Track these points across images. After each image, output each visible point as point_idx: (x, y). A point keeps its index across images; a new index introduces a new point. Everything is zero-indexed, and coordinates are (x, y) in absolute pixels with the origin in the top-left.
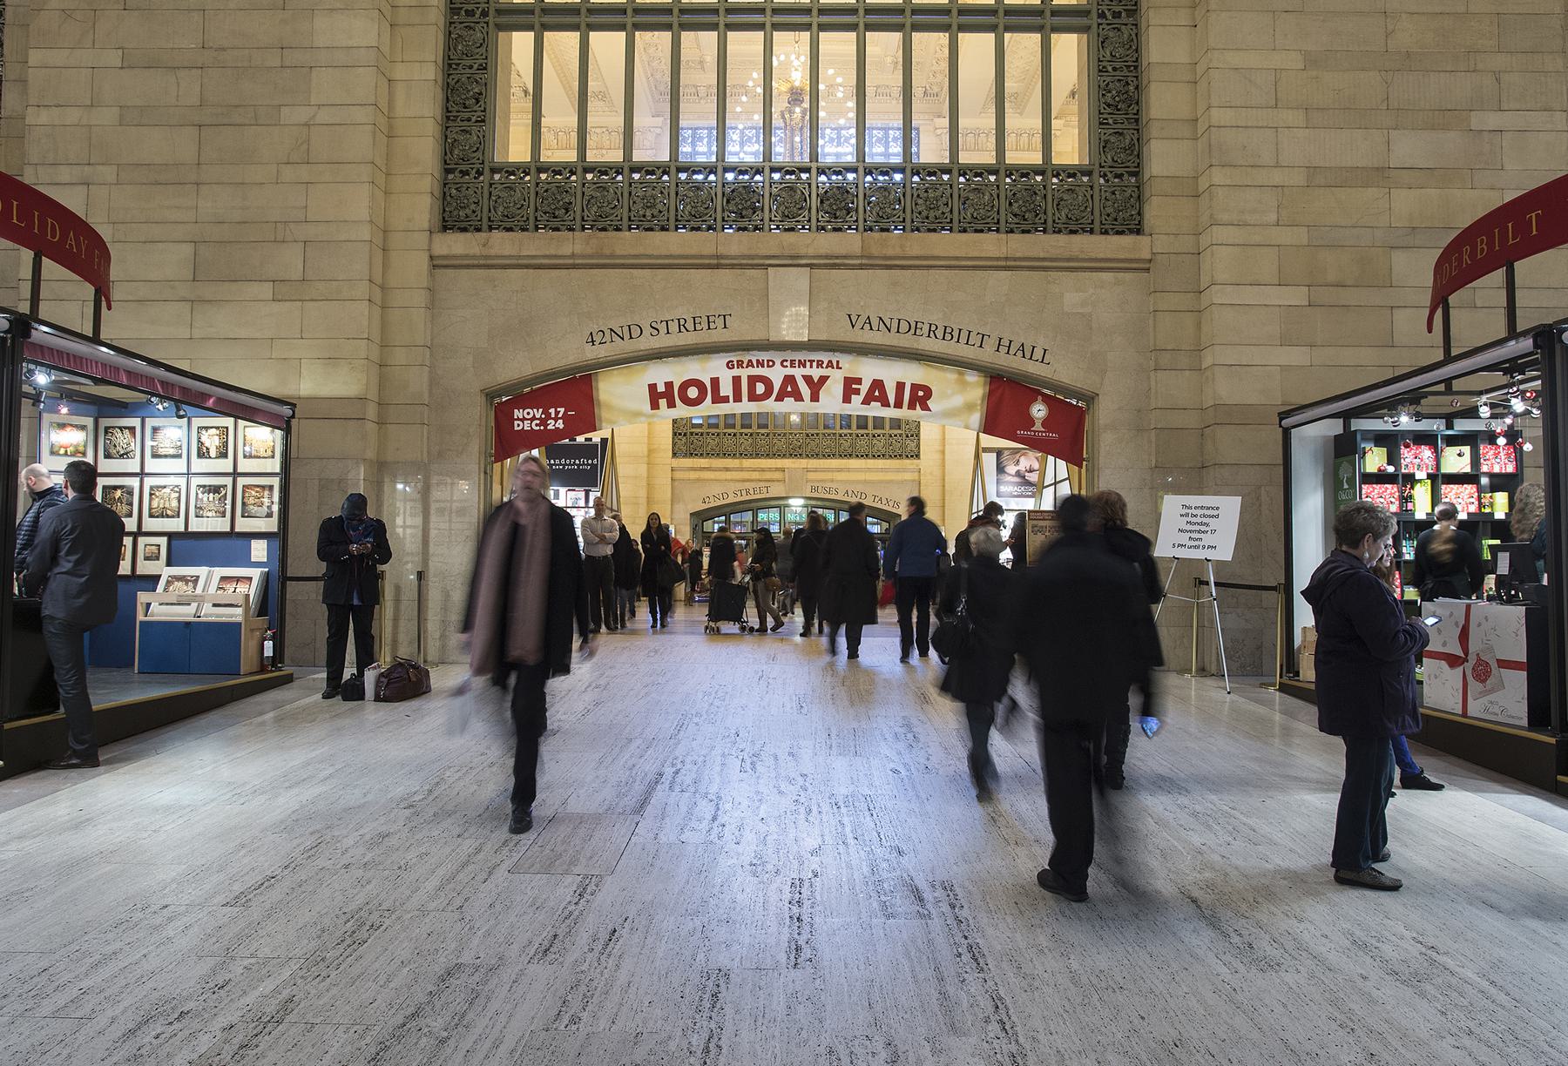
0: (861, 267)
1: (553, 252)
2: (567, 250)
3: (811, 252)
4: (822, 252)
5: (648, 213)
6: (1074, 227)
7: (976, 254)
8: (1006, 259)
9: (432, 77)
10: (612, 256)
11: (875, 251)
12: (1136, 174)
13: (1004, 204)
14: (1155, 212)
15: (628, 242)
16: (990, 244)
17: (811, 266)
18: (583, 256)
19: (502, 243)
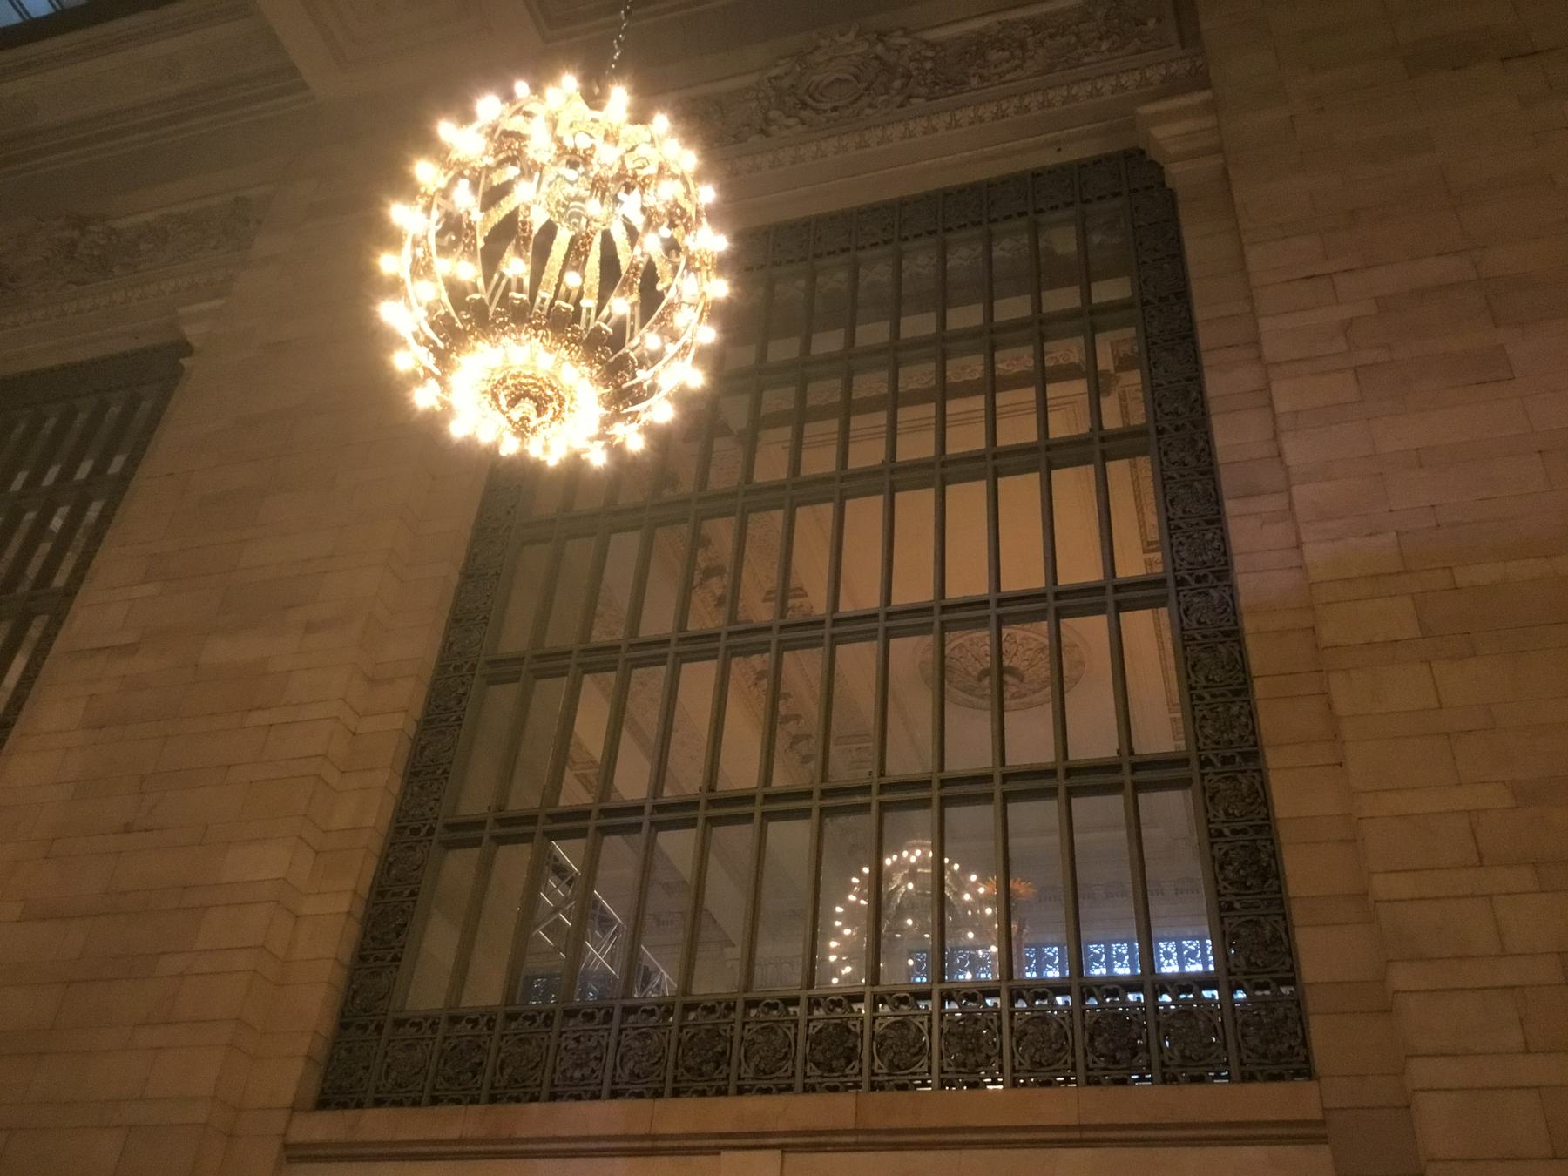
0: (857, 1147)
1: (435, 1135)
2: (453, 1132)
3: (782, 1126)
4: (800, 1126)
5: (577, 1074)
6: (1191, 1068)
7: (1029, 1122)
8: (1081, 1127)
9: (345, 908)
10: (512, 1140)
11: (875, 1122)
12: (1291, 982)
13: (1080, 1039)
14: (1322, 1035)
15: (535, 1119)
16: (1065, 1102)
17: (784, 1148)
18: (474, 1141)
19: (376, 1124)
